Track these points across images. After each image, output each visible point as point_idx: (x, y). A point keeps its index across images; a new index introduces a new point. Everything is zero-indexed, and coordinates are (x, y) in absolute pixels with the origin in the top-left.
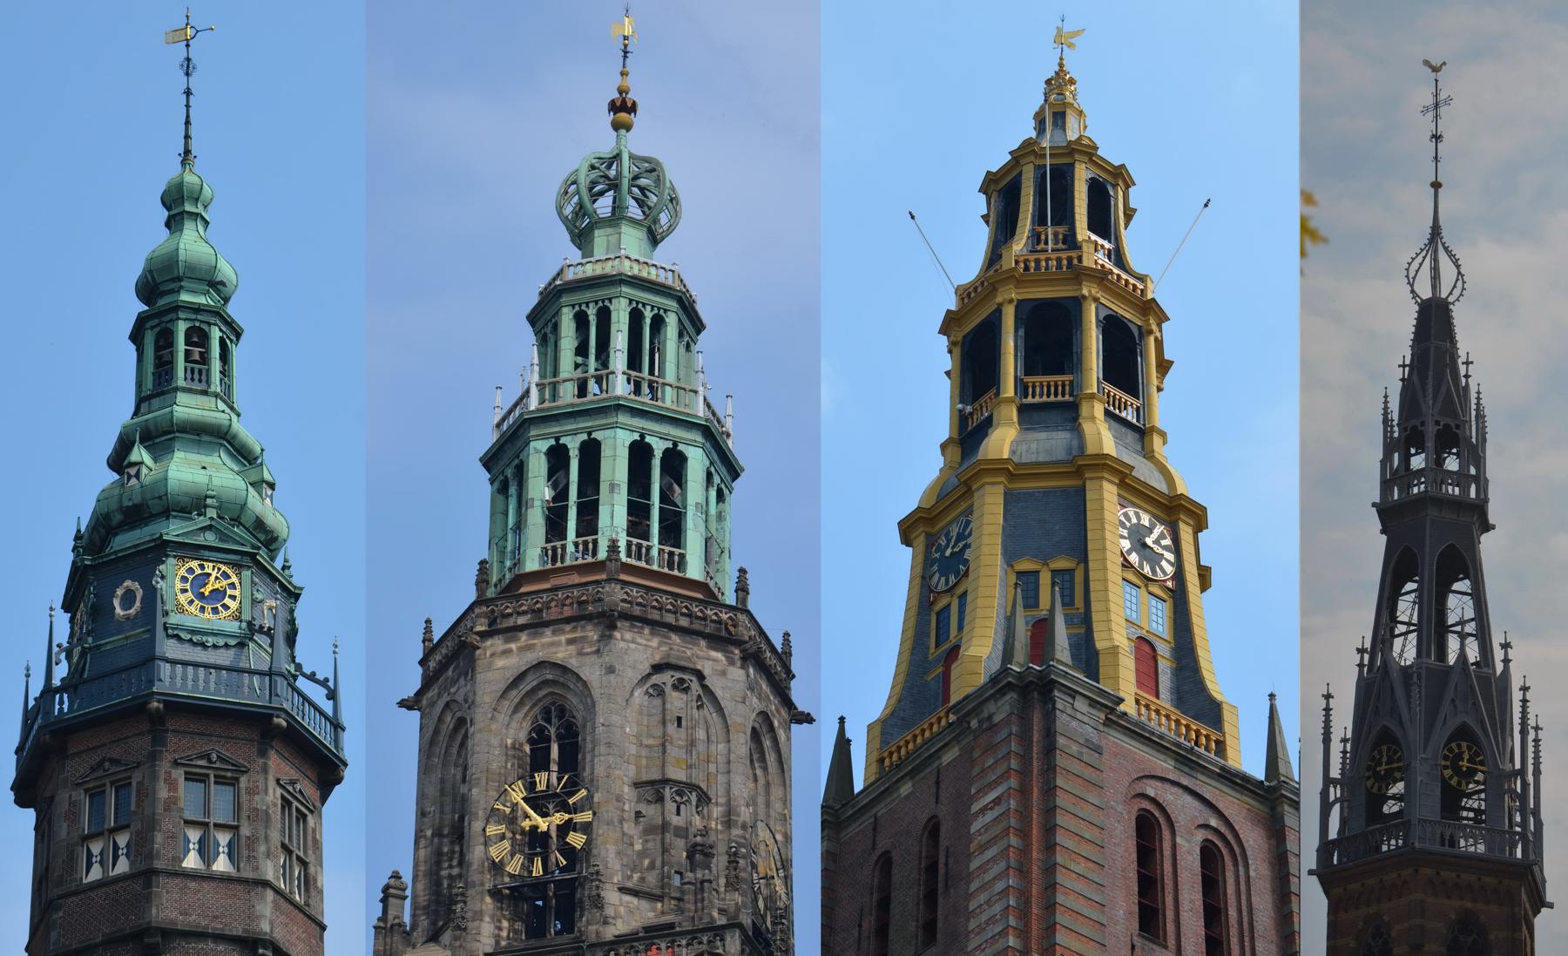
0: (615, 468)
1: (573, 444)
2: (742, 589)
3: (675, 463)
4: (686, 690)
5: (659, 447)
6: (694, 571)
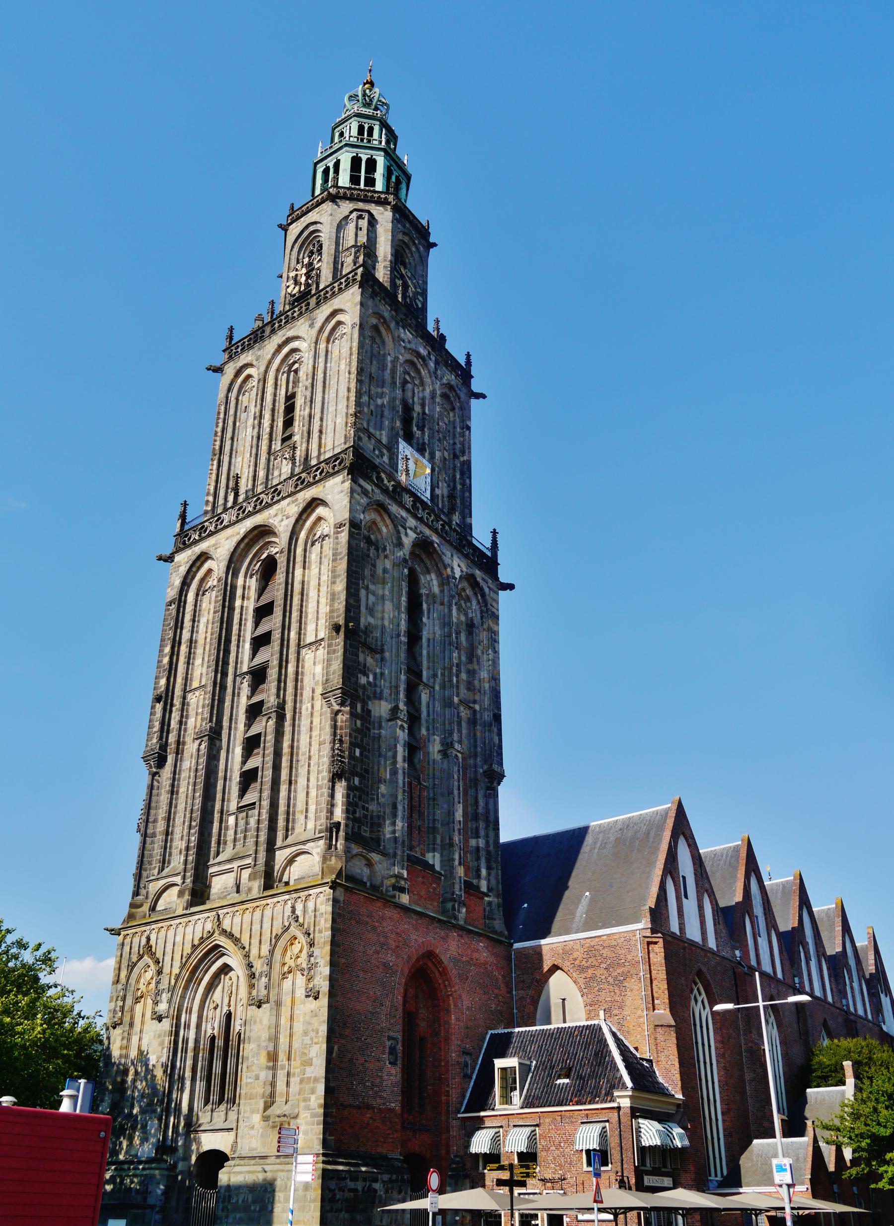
1: (331, 165)
3: (371, 165)
4: (363, 219)
5: (364, 158)
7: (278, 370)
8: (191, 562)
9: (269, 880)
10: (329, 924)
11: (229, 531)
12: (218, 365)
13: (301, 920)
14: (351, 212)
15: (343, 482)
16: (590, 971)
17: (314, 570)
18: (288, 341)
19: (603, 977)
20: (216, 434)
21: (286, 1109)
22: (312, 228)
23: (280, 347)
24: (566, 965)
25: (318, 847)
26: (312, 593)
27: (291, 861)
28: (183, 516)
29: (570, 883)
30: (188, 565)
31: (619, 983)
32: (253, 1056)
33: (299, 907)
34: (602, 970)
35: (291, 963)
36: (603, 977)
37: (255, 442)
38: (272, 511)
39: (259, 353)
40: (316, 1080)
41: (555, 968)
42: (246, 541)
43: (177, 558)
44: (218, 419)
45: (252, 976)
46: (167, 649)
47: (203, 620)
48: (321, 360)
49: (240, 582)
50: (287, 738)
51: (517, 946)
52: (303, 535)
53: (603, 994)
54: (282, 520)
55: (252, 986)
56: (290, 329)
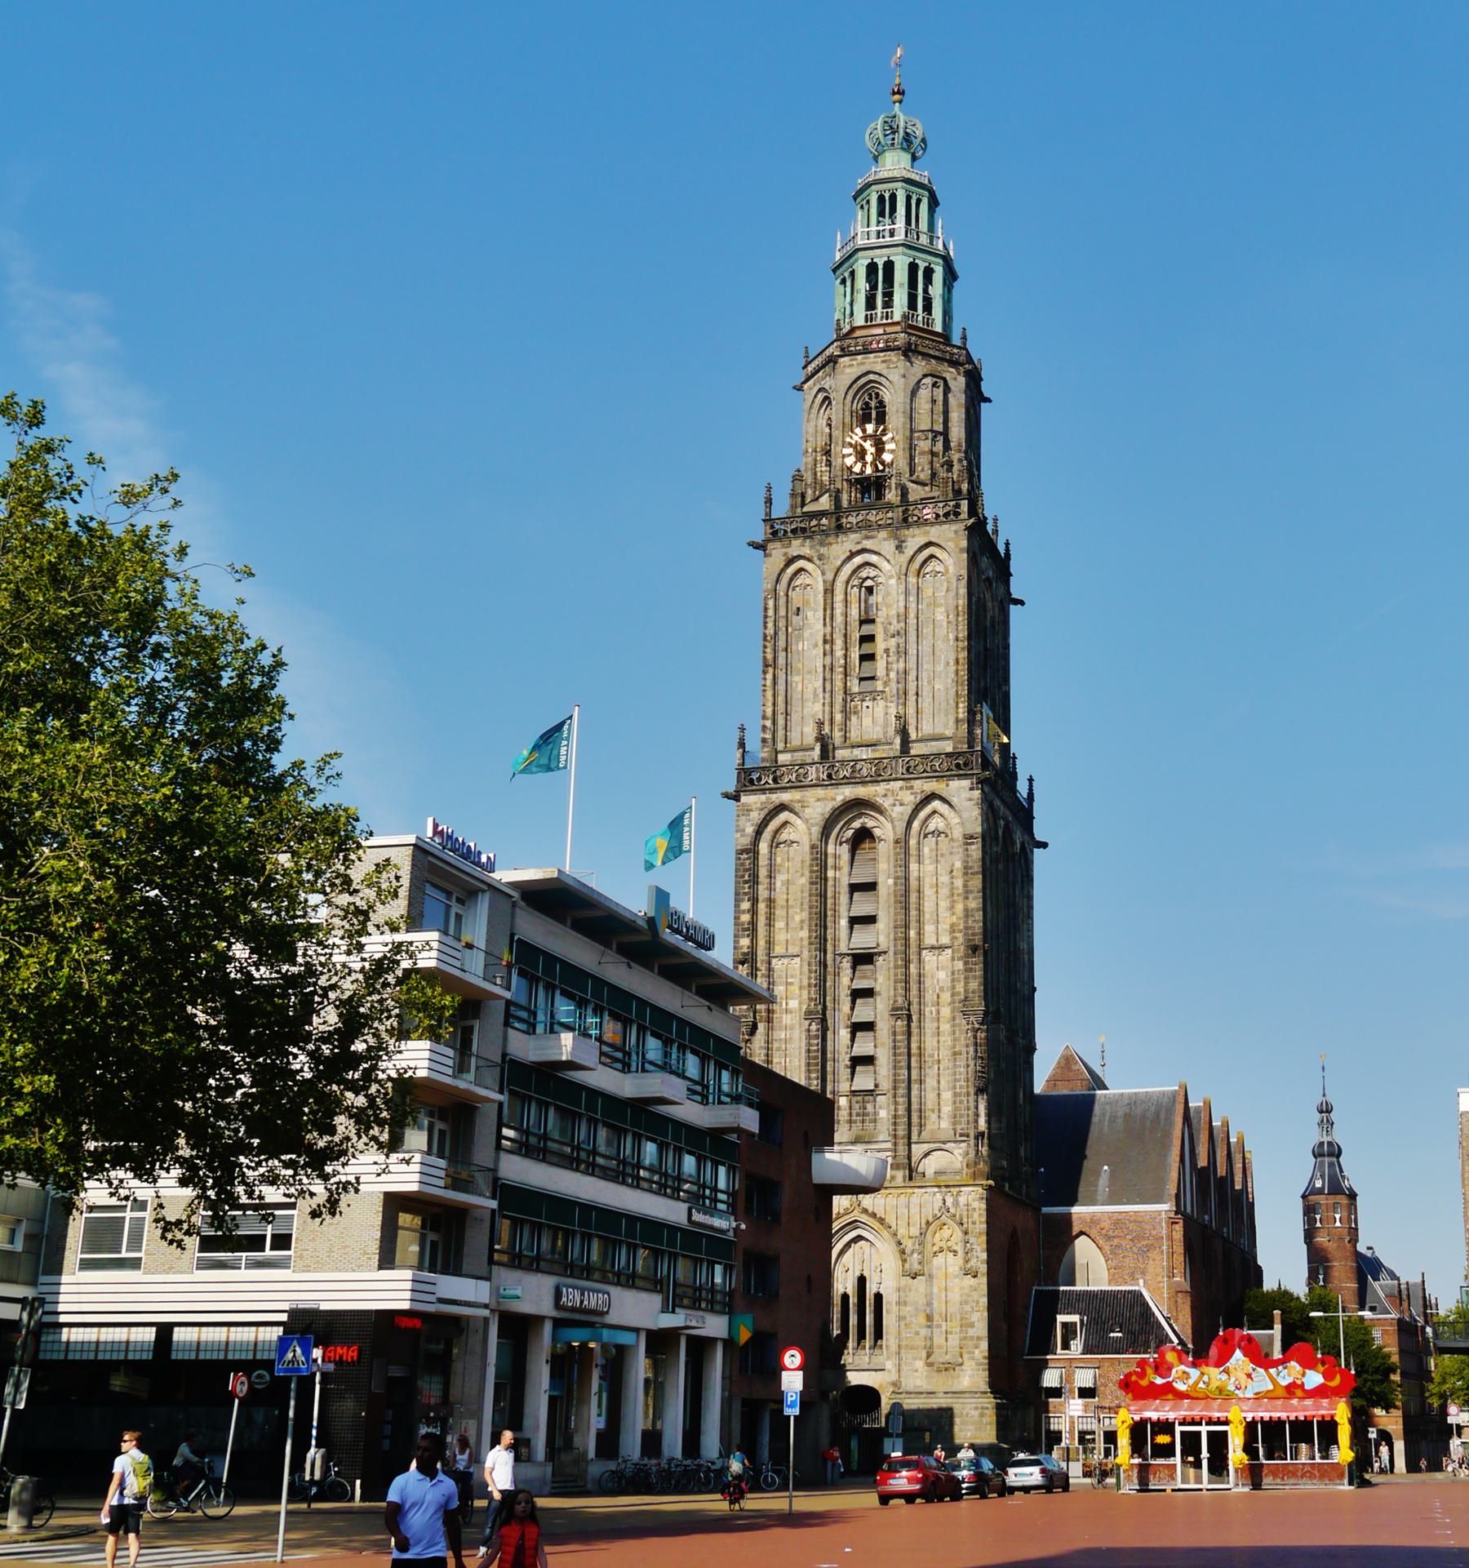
0: (901, 276)
1: (880, 263)
2: (964, 338)
3: (929, 272)
5: (922, 265)
6: (938, 328)
7: (847, 582)
9: (911, 1172)
10: (984, 1219)
11: (820, 792)
12: (759, 539)
13: (952, 1210)
14: (925, 376)
15: (972, 789)
16: (1116, 1241)
17: (928, 867)
18: (863, 551)
20: (765, 639)
21: (948, 1358)
22: (872, 377)
23: (853, 555)
24: (1094, 1233)
26: (928, 892)
27: (927, 1155)
28: (742, 745)
29: (1088, 1152)
31: (1144, 1252)
33: (949, 1201)
35: (942, 1244)
37: (828, 676)
38: (881, 788)
39: (823, 550)
40: (979, 1338)
41: (1082, 1233)
43: (744, 799)
44: (766, 617)
45: (903, 1252)
46: (746, 905)
47: (780, 879)
48: (912, 599)
49: (831, 849)
50: (914, 1039)
51: (1045, 1210)
52: (916, 824)
55: (904, 1261)
56: (867, 538)
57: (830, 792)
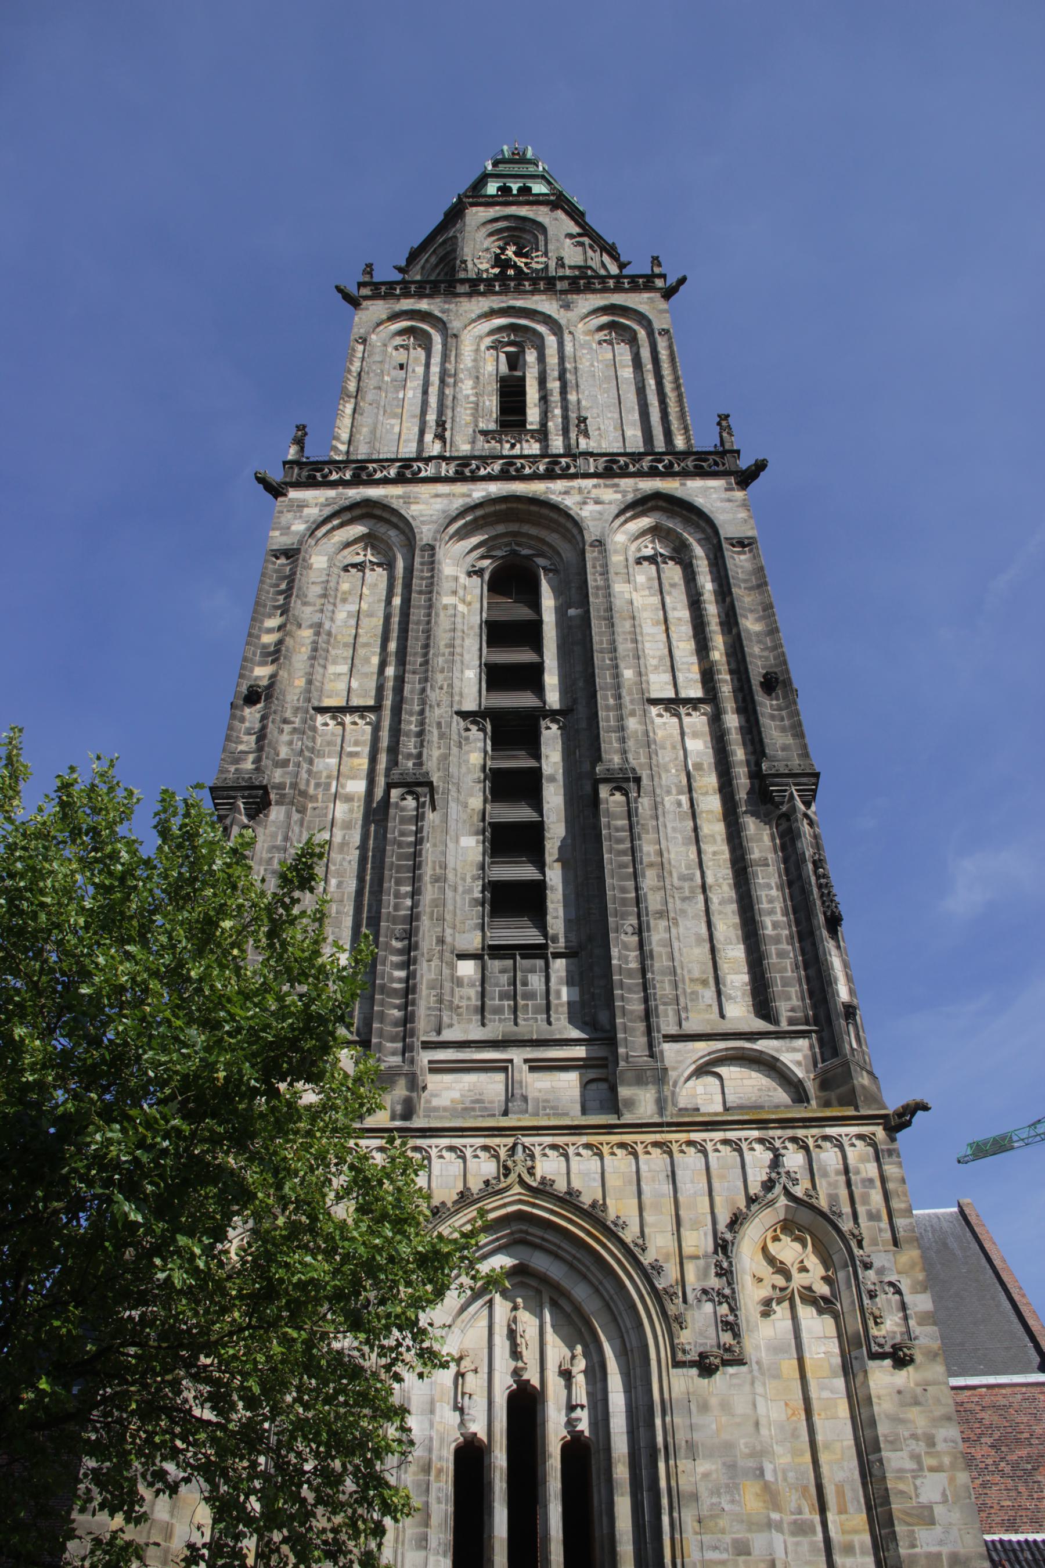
8: (336, 507)
19: (989, 1461)
23: (492, 313)
25: (795, 1050)
30: (327, 511)
32: (716, 1492)
33: (794, 1160)
34: (986, 1448)
36: (989, 1461)
42: (479, 512)
53: (993, 1491)
54: (585, 503)
57: (460, 488)
